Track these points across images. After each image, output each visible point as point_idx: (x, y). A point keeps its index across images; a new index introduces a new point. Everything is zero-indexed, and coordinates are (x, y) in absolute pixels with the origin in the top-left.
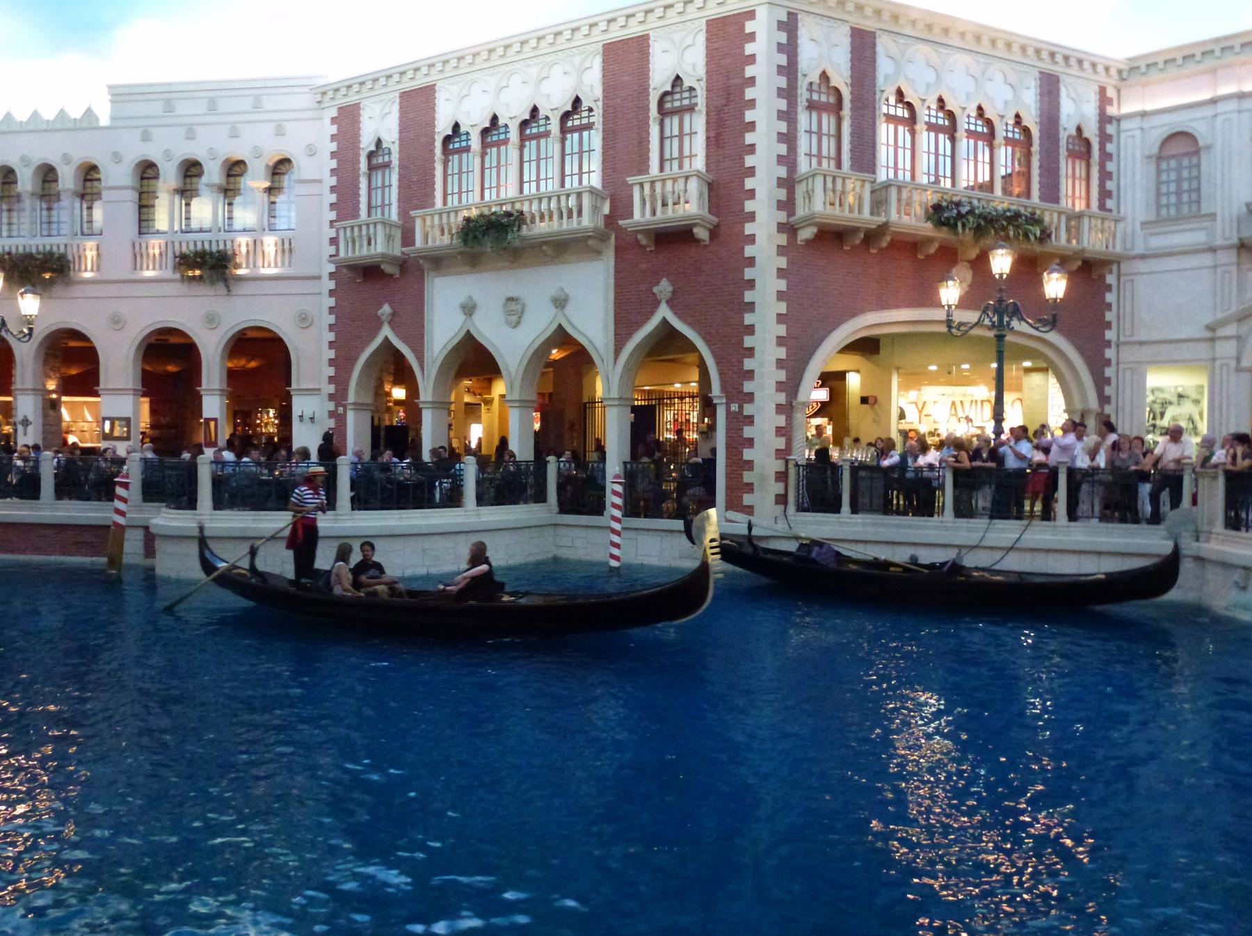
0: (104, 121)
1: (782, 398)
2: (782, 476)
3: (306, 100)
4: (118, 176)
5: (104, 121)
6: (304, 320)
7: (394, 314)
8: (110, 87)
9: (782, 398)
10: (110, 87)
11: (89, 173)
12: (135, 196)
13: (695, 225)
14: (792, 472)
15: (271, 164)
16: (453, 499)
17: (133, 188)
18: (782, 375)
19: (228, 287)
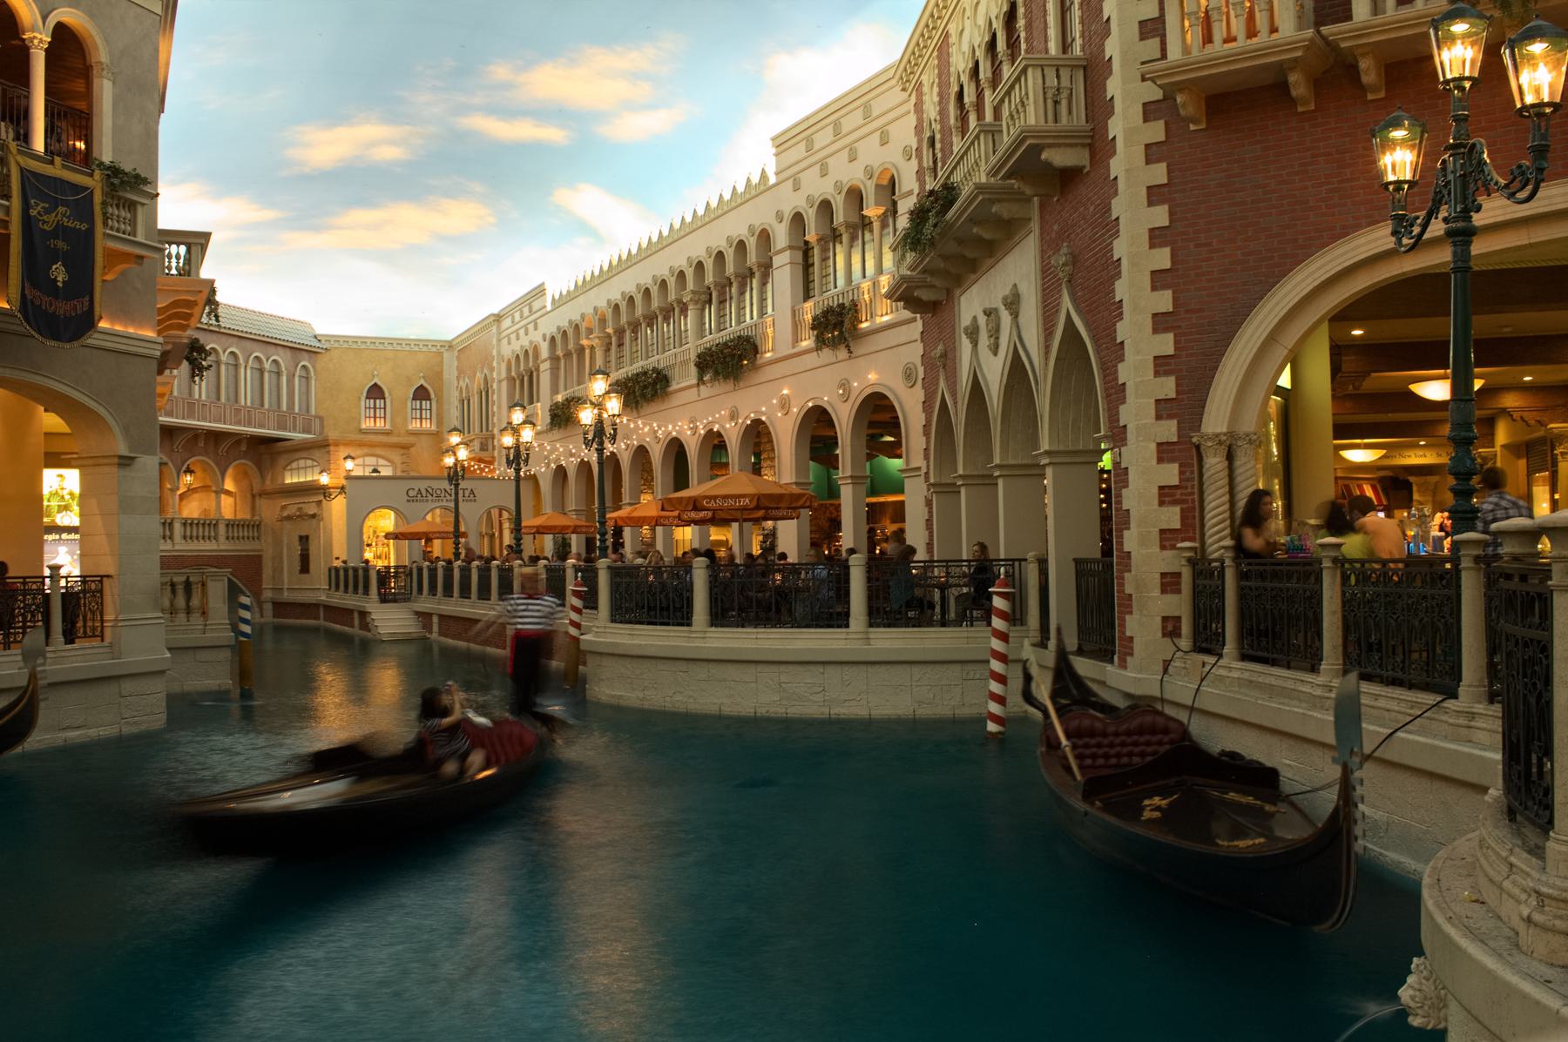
0: (772, 180)
1: (1169, 430)
2: (1170, 583)
3: (896, 96)
4: (781, 236)
5: (772, 180)
6: (909, 375)
7: (944, 355)
8: (773, 139)
9: (1169, 430)
10: (773, 139)
11: (765, 237)
12: (799, 255)
13: (1038, 149)
14: (1186, 574)
15: (885, 182)
16: (839, 619)
17: (791, 247)
18: (1167, 387)
19: (848, 347)
